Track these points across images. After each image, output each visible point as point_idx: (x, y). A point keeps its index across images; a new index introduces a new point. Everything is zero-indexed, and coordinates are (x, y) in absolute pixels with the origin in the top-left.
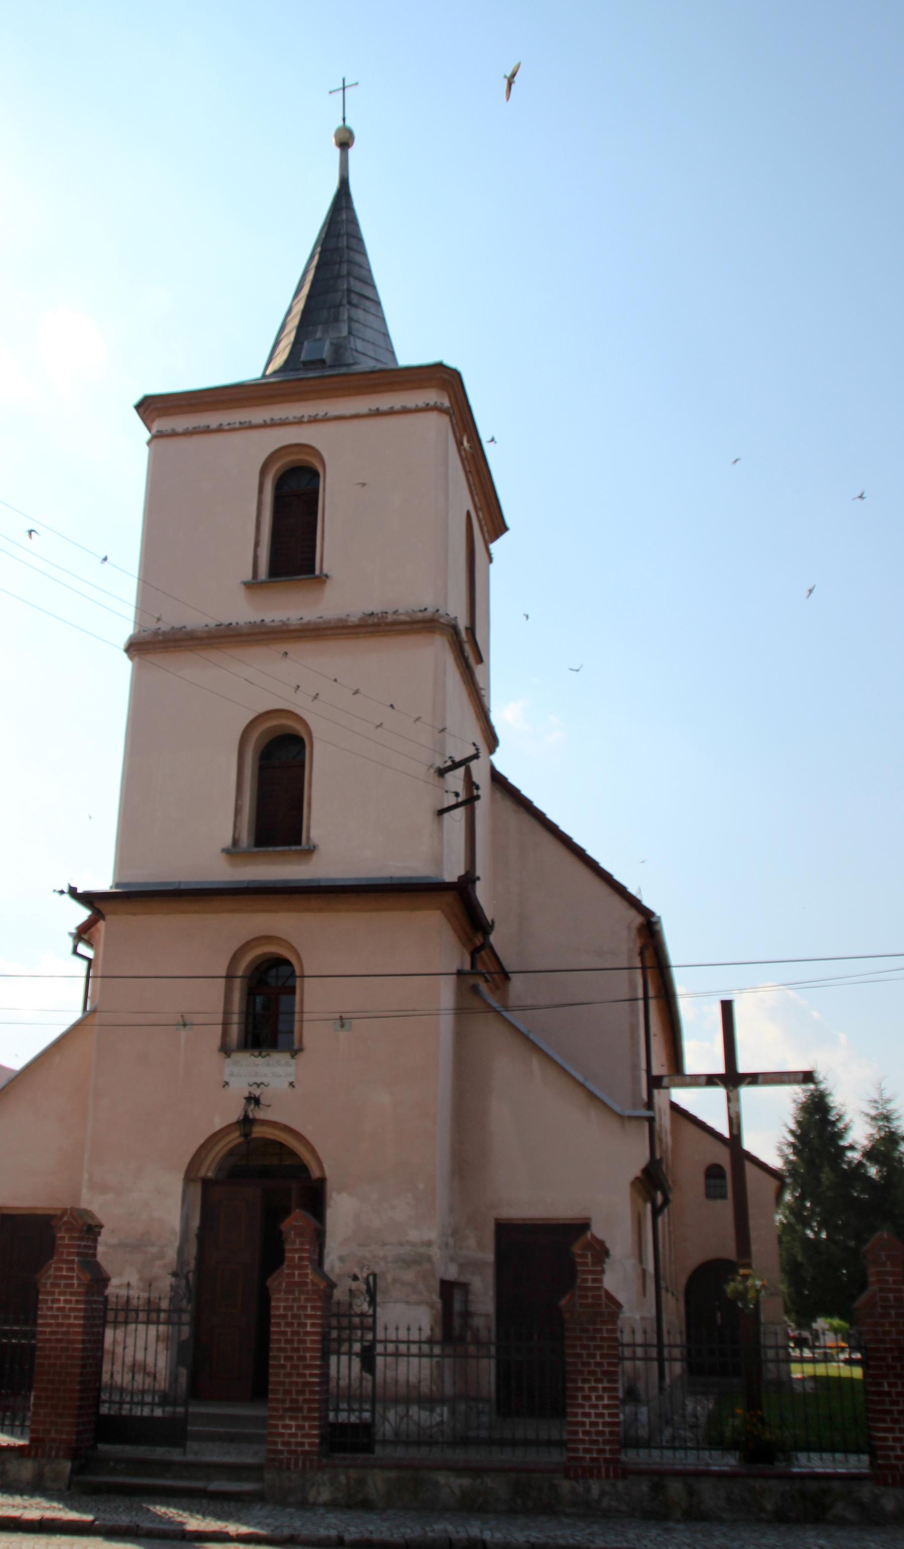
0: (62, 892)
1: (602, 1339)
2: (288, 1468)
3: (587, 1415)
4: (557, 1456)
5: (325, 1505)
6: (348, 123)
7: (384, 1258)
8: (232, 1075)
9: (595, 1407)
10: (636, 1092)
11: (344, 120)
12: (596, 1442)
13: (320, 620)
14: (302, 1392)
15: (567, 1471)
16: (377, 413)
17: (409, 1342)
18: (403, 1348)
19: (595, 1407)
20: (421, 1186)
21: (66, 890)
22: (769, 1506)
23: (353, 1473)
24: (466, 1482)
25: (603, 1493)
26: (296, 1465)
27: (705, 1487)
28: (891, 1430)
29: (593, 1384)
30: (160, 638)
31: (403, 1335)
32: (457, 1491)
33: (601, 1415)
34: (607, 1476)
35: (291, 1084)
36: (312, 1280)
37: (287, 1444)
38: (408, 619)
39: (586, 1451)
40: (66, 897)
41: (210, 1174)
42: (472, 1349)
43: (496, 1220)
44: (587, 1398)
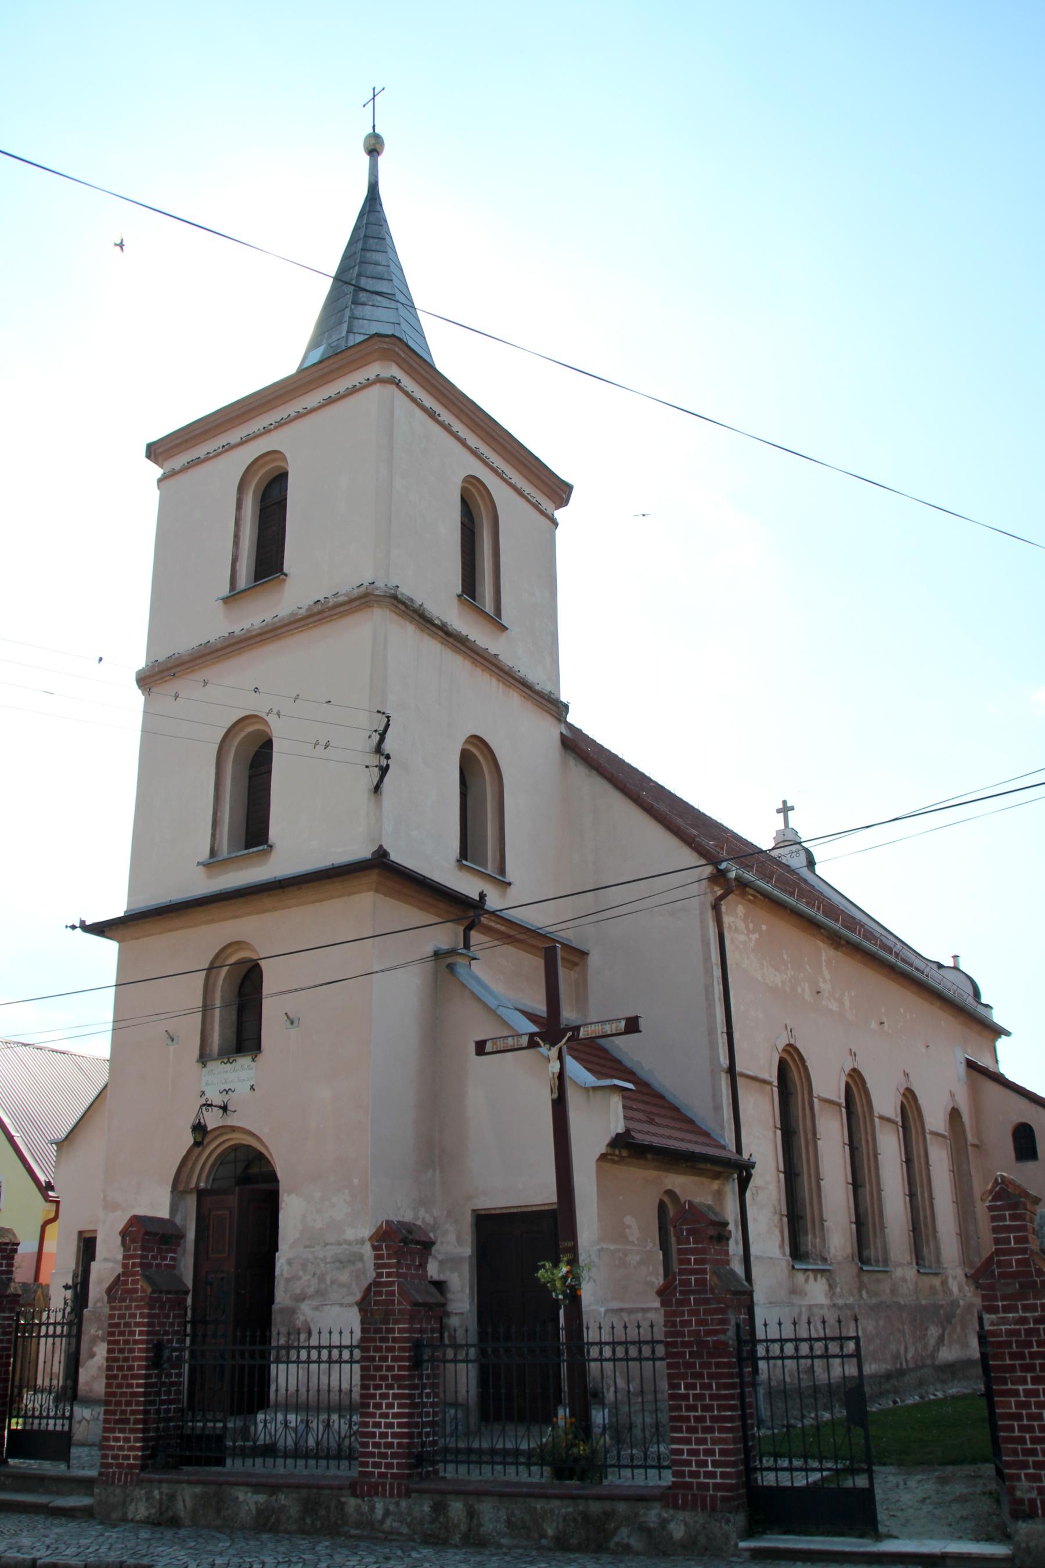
0: (73, 927)
1: (395, 1340)
2: (113, 1482)
3: (377, 1425)
4: (345, 1471)
5: (140, 1521)
6: (376, 131)
7: (324, 1259)
8: (207, 1084)
9: (385, 1416)
10: (714, 1060)
11: (374, 127)
12: (384, 1456)
13: (276, 619)
14: (129, 1403)
15: (353, 1488)
16: (330, 401)
17: (782, 1341)
18: (834, 1348)
19: (385, 1416)
20: (356, 1181)
21: (77, 924)
22: (550, 1532)
23: (166, 1488)
24: (261, 1498)
25: (387, 1513)
26: (120, 1480)
27: (486, 1508)
28: (687, 1441)
29: (384, 1391)
30: (157, 669)
31: (336, 1341)
32: (253, 1507)
33: (390, 1425)
34: (392, 1495)
35: (252, 1088)
36: (142, 1287)
37: (115, 1457)
38: (346, 599)
39: (376, 1465)
40: (78, 930)
41: (202, 1185)
42: (450, 1353)
43: (474, 1211)
44: (378, 1406)
